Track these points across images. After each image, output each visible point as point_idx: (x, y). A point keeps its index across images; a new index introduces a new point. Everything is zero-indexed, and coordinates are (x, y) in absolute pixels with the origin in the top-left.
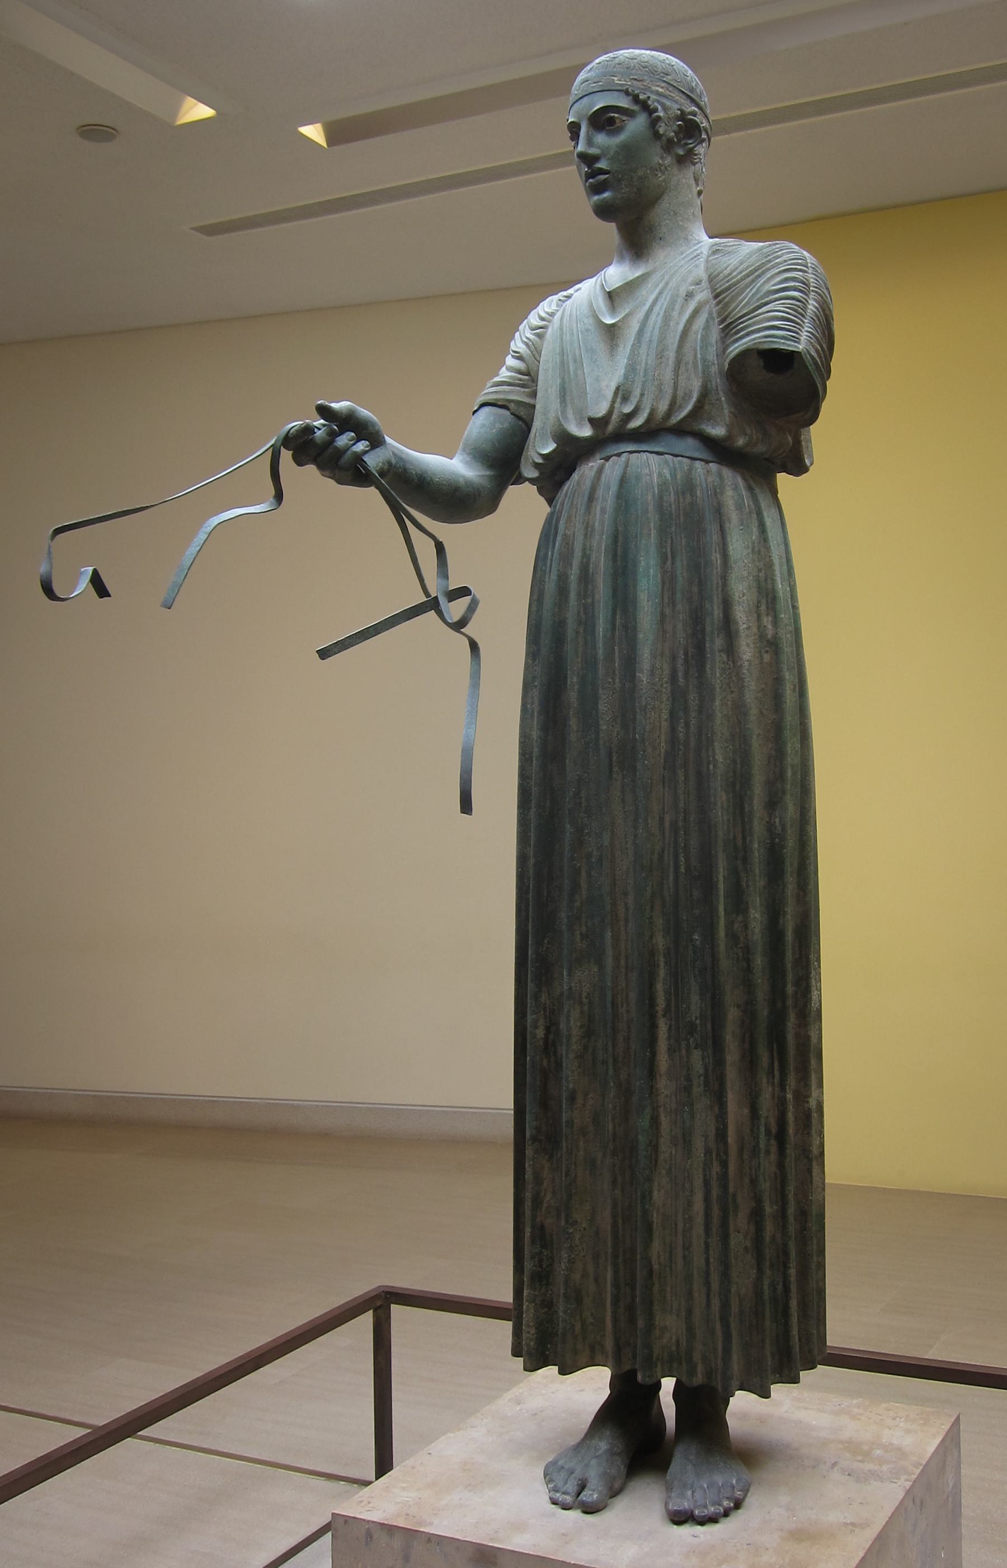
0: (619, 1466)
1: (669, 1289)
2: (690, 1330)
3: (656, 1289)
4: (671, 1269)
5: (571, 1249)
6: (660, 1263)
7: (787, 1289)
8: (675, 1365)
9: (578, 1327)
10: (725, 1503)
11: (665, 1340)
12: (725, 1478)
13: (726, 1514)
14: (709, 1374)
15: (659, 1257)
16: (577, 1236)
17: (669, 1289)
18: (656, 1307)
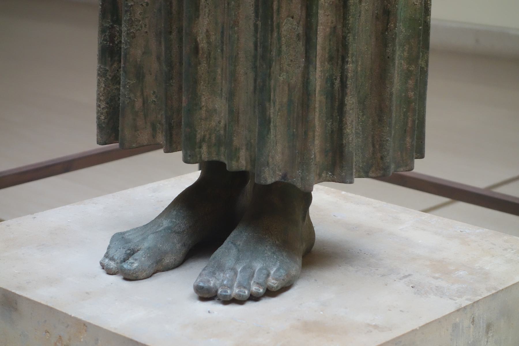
0: (175, 247)
1: (219, 71)
2: (233, 114)
3: (203, 67)
4: (222, 50)
5: (131, 23)
6: (209, 43)
7: (343, 85)
8: (222, 149)
9: (138, 104)
10: (254, 288)
11: (213, 124)
12: (269, 267)
13: (254, 298)
14: (253, 161)
15: (208, 36)
16: (139, 10)
17: (219, 71)
18: (202, 87)
